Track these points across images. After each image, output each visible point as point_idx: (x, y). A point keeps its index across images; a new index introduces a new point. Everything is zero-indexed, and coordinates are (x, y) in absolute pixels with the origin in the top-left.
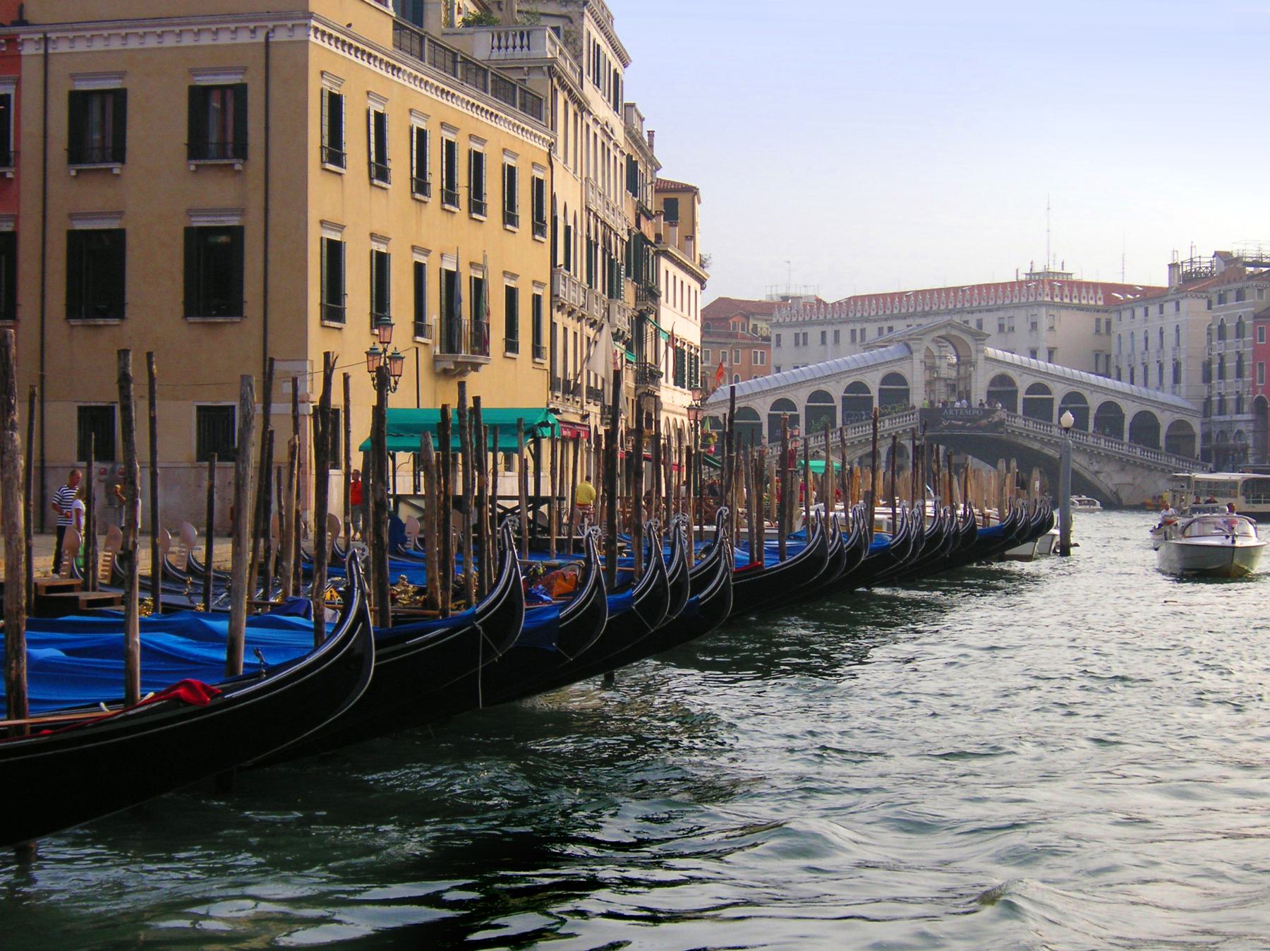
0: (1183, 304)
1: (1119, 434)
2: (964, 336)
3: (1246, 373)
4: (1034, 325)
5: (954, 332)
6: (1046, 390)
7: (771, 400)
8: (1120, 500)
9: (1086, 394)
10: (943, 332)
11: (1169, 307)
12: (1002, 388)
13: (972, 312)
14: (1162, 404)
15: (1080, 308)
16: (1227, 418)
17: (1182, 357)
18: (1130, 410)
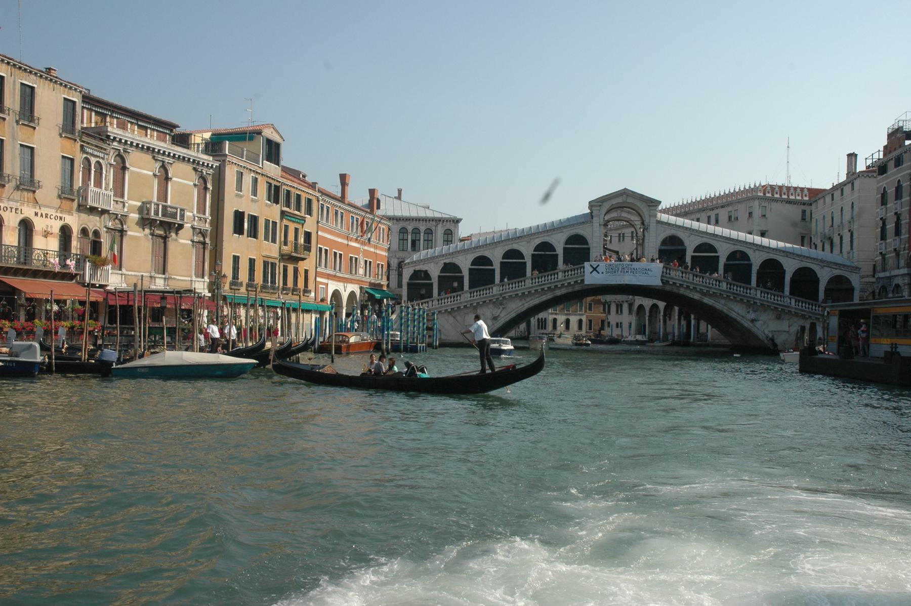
0: (857, 183)
1: (780, 286)
2: (639, 204)
3: (903, 231)
4: (750, 214)
5: (630, 200)
6: (712, 249)
7: (471, 257)
8: (775, 345)
9: (750, 253)
10: (619, 200)
11: (847, 189)
12: (671, 250)
13: (713, 209)
14: (822, 261)
15: (789, 202)
16: (887, 274)
17: (855, 227)
18: (790, 267)
